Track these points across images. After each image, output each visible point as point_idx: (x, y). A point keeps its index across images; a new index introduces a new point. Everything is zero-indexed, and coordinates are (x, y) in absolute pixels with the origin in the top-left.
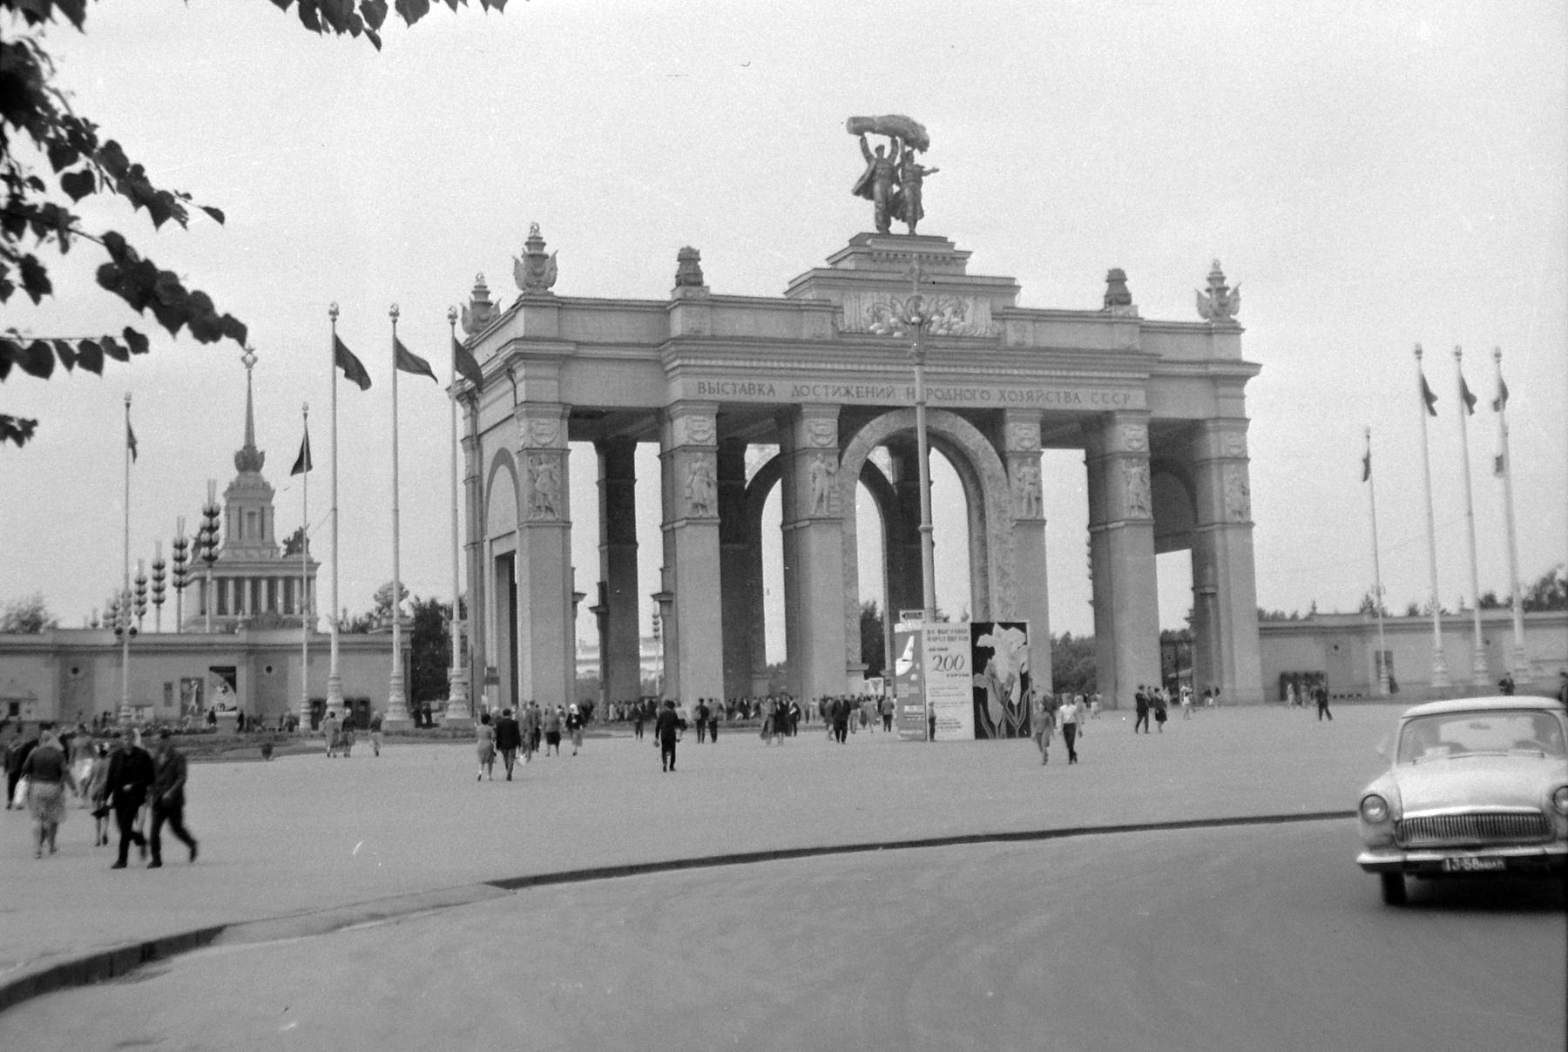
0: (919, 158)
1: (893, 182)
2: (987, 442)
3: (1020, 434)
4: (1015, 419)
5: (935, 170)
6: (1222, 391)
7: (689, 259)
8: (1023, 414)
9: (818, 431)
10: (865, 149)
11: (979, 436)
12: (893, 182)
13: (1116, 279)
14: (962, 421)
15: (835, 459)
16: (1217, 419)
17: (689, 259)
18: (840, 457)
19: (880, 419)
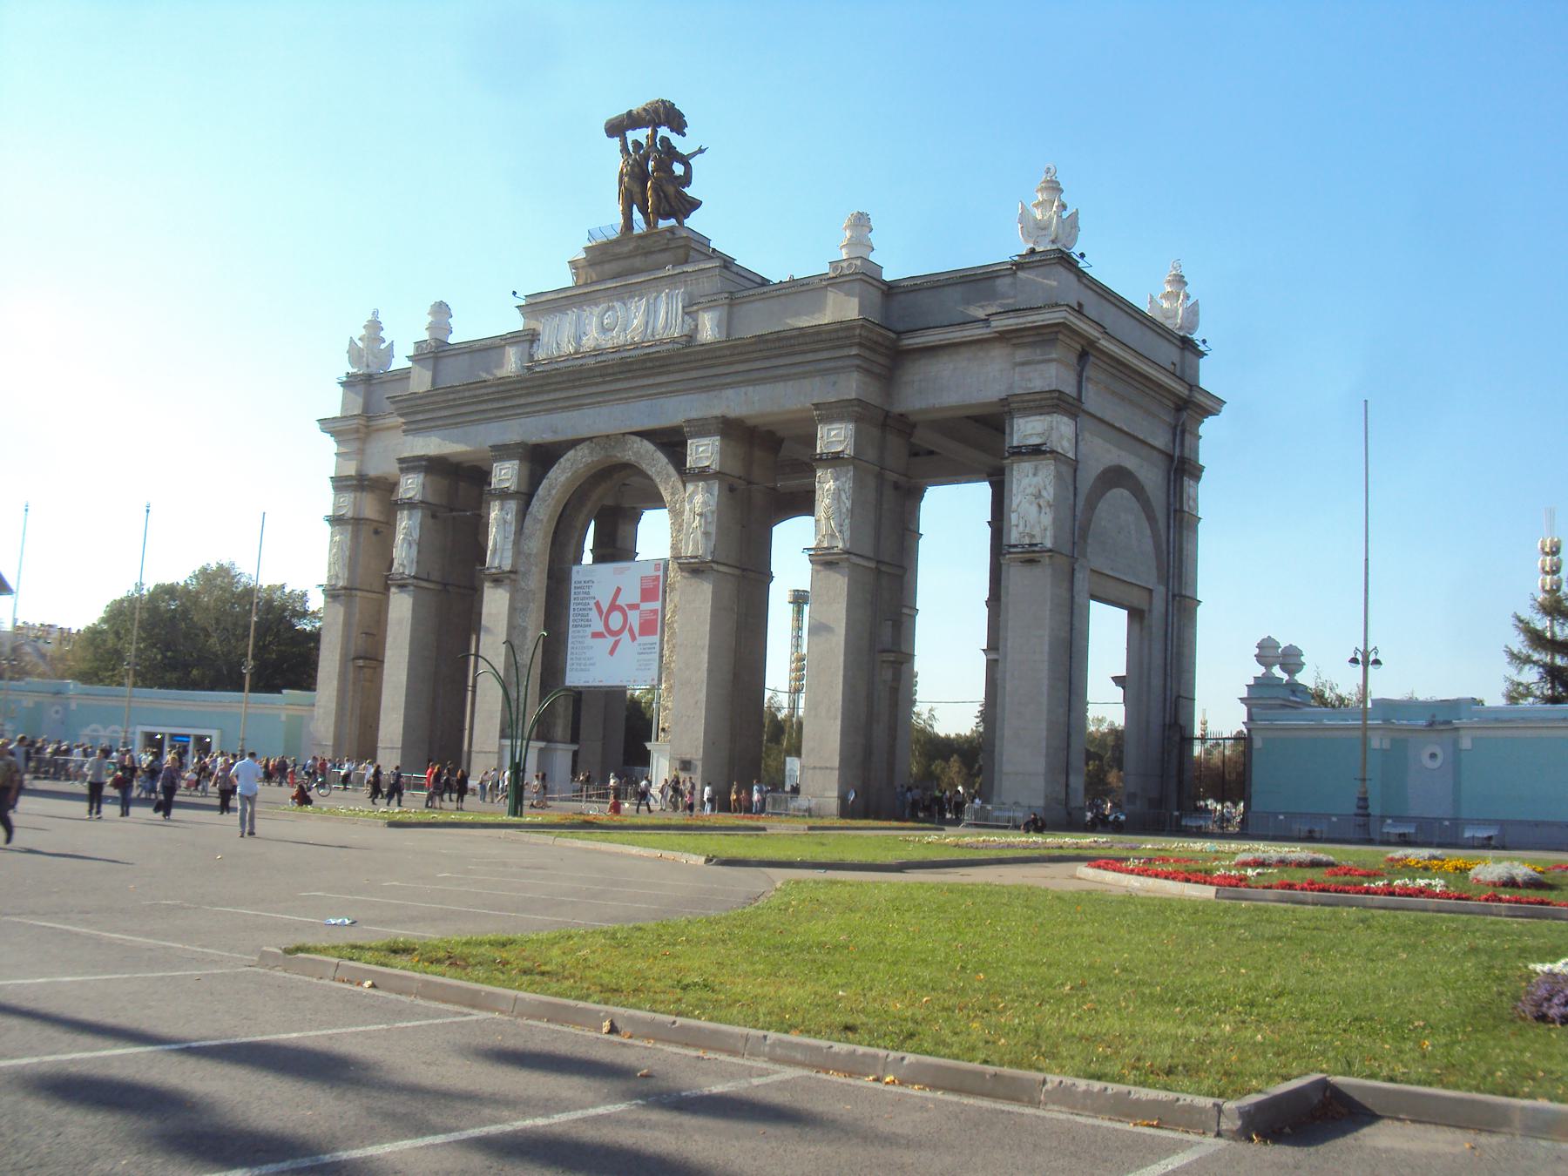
0: (675, 139)
1: (657, 180)
2: (671, 470)
3: (703, 452)
4: (692, 437)
5: (701, 151)
6: (1021, 354)
7: (441, 310)
8: (702, 428)
9: (506, 474)
10: (624, 149)
11: (662, 459)
12: (657, 180)
13: (861, 222)
14: (647, 446)
15: (512, 505)
16: (1004, 401)
17: (441, 310)
18: (528, 504)
19: (571, 453)
